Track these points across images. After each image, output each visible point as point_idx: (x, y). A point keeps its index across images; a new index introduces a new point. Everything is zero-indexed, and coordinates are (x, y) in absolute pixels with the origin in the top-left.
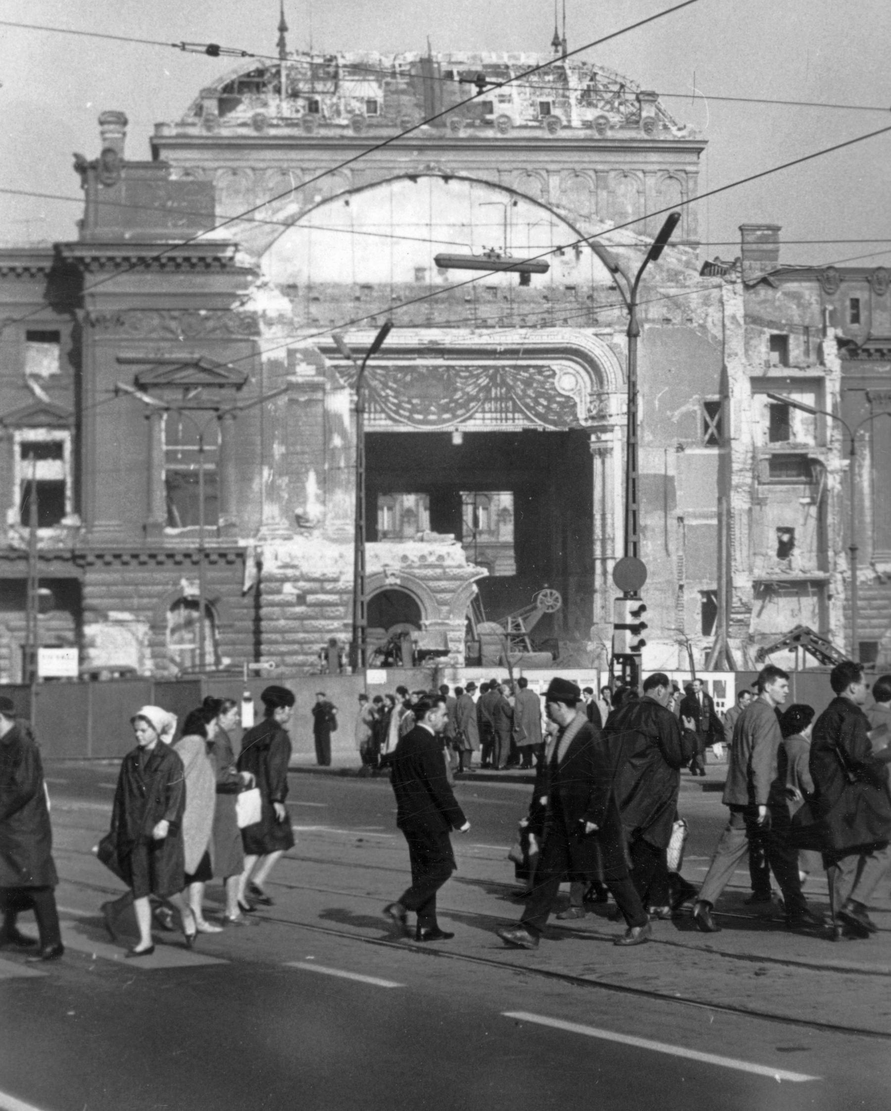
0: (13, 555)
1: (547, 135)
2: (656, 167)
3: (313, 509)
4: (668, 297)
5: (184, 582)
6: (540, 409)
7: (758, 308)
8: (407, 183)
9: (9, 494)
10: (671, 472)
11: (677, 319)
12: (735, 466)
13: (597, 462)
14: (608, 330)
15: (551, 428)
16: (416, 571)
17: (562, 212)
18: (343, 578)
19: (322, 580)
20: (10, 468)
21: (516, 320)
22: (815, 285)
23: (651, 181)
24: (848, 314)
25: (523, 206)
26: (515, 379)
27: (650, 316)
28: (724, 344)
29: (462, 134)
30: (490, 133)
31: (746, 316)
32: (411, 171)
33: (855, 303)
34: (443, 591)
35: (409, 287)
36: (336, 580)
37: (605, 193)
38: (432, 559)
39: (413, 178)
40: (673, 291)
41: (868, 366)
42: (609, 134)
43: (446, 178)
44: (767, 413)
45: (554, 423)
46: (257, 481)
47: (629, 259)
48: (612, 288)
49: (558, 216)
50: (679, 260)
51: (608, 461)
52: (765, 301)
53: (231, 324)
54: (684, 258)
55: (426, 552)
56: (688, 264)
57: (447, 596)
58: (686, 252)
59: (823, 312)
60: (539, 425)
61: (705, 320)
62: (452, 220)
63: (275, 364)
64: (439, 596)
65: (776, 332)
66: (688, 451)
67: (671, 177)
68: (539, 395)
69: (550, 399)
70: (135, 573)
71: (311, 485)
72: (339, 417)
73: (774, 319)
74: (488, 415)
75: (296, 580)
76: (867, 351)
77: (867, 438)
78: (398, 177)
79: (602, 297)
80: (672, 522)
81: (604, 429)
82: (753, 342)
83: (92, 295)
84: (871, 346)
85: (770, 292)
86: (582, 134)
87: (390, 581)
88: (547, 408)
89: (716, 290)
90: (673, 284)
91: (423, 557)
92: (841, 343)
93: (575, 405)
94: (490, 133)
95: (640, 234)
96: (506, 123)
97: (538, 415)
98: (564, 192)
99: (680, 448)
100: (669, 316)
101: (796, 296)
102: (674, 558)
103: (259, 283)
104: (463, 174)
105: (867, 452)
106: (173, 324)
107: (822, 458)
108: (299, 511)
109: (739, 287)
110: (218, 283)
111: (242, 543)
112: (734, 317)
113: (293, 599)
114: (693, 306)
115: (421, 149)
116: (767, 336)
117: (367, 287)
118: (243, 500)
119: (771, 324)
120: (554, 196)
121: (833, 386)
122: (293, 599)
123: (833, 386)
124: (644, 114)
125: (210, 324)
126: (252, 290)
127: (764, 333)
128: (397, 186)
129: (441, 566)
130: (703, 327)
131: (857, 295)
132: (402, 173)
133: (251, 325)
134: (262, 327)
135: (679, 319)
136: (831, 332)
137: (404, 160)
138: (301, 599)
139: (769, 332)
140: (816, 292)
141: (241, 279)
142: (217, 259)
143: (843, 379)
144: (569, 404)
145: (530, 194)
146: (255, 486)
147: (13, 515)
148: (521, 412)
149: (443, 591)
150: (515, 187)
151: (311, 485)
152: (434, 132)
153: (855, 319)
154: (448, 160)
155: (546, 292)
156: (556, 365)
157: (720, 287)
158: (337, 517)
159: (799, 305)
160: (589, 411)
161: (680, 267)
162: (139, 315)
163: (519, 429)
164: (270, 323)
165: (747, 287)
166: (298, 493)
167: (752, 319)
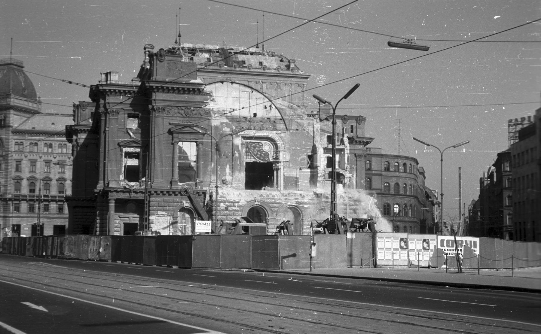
0: (125, 191)
1: (263, 71)
2: (295, 83)
3: (228, 178)
5: (184, 202)
6: (258, 156)
9: (121, 170)
10: (298, 176)
11: (300, 130)
12: (319, 175)
13: (275, 172)
14: (280, 132)
15: (261, 161)
16: (266, 200)
17: (267, 95)
18: (241, 202)
19: (234, 202)
20: (121, 161)
21: (252, 128)
22: (341, 121)
24: (350, 130)
25: (255, 93)
26: (251, 146)
28: (314, 137)
29: (238, 69)
30: (246, 70)
31: (320, 129)
32: (222, 80)
33: (352, 127)
34: (274, 207)
36: (238, 202)
38: (270, 196)
39: (222, 82)
40: (299, 121)
41: (356, 146)
42: (281, 72)
43: (232, 83)
44: (326, 159)
45: (262, 160)
46: (209, 167)
48: (281, 119)
49: (265, 96)
51: (279, 172)
53: (202, 113)
55: (268, 194)
56: (304, 113)
57: (276, 209)
59: (343, 129)
60: (258, 160)
63: (216, 127)
64: (273, 209)
65: (329, 134)
66: (303, 170)
68: (258, 151)
69: (261, 153)
70: (167, 198)
71: (228, 170)
72: (238, 146)
75: (224, 202)
76: (356, 141)
78: (217, 82)
79: (277, 121)
81: (278, 162)
83: (155, 100)
84: (358, 140)
85: (327, 122)
86: (273, 71)
87: (257, 203)
88: (260, 155)
91: (268, 195)
92: (349, 138)
93: (269, 155)
94: (246, 70)
96: (250, 67)
97: (257, 157)
98: (267, 89)
99: (301, 169)
103: (211, 99)
104: (237, 82)
105: (355, 172)
106: (182, 112)
107: (344, 173)
108: (223, 178)
109: (318, 120)
110: (198, 98)
111: (204, 189)
113: (224, 208)
115: (225, 73)
118: (205, 173)
119: (328, 132)
120: (264, 90)
121: (347, 151)
122: (224, 208)
123: (347, 151)
124: (291, 66)
125: (195, 112)
126: (209, 101)
128: (217, 85)
129: (273, 199)
130: (308, 132)
131: (353, 124)
132: (219, 80)
133: (208, 113)
134: (212, 114)
136: (346, 135)
137: (220, 77)
138: (227, 209)
139: (327, 135)
141: (205, 97)
142: (199, 89)
143: (350, 150)
144: (267, 155)
145: (257, 89)
146: (209, 169)
147: (122, 177)
148: (252, 156)
149: (274, 207)
150: (253, 87)
151: (228, 170)
152: (229, 68)
153: (352, 131)
154: (233, 77)
155: (261, 120)
156: (263, 142)
157: (313, 120)
158: (236, 181)
160: (273, 157)
162: (170, 108)
163: (252, 161)
164: (214, 113)
165: (321, 120)
166: (224, 171)
167: (322, 130)
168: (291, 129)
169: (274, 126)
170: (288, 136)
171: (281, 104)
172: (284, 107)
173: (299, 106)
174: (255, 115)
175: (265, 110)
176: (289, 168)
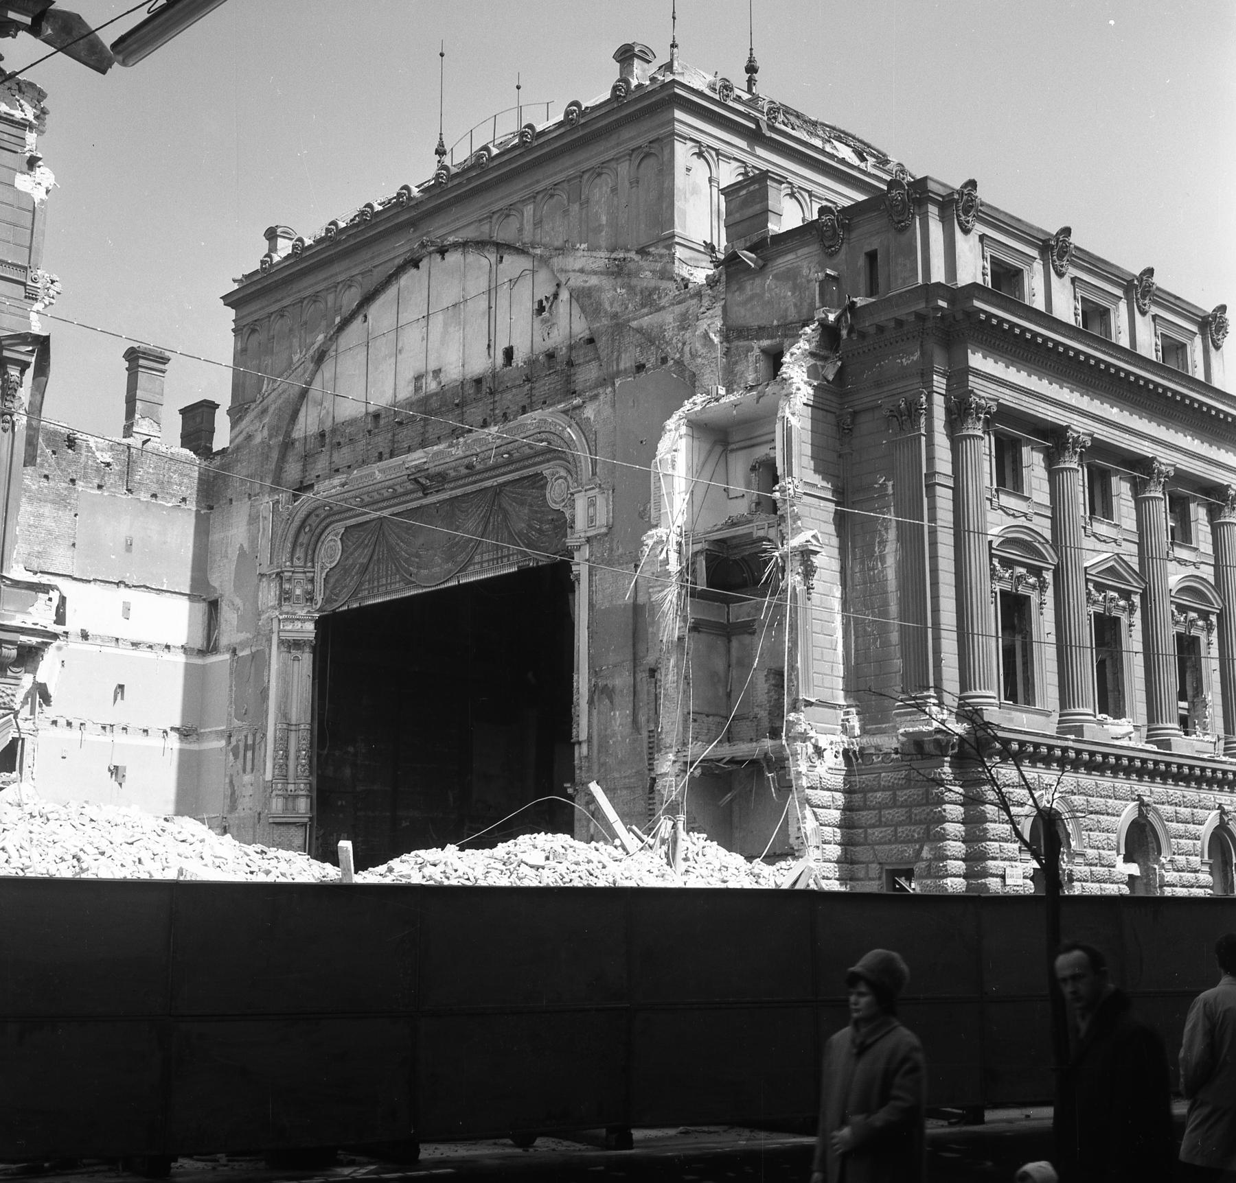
4: (639, 330)
7: (743, 312)
8: (413, 271)
23: (624, 168)
27: (622, 367)
35: (410, 404)
37: (576, 207)
40: (646, 321)
43: (442, 252)
47: (599, 289)
52: (751, 298)
54: (659, 266)
58: (661, 256)
61: (682, 352)
65: (765, 343)
67: (648, 155)
73: (763, 323)
74: (486, 557)
77: (890, 491)
80: (643, 676)
82: (738, 368)
89: (694, 301)
90: (645, 310)
95: (612, 252)
100: (642, 360)
101: (790, 276)
102: (645, 734)
114: (668, 335)
116: (757, 352)
117: (376, 416)
119: (761, 332)
127: (751, 349)
135: (653, 360)
137: (401, 247)
159: (794, 289)
161: (653, 283)
167: (732, 333)
168: (618, 374)
169: (569, 380)
170: (607, 411)
171: (582, 271)
172: (594, 281)
173: (643, 252)
174: (509, 353)
175: (538, 320)
176: (610, 563)
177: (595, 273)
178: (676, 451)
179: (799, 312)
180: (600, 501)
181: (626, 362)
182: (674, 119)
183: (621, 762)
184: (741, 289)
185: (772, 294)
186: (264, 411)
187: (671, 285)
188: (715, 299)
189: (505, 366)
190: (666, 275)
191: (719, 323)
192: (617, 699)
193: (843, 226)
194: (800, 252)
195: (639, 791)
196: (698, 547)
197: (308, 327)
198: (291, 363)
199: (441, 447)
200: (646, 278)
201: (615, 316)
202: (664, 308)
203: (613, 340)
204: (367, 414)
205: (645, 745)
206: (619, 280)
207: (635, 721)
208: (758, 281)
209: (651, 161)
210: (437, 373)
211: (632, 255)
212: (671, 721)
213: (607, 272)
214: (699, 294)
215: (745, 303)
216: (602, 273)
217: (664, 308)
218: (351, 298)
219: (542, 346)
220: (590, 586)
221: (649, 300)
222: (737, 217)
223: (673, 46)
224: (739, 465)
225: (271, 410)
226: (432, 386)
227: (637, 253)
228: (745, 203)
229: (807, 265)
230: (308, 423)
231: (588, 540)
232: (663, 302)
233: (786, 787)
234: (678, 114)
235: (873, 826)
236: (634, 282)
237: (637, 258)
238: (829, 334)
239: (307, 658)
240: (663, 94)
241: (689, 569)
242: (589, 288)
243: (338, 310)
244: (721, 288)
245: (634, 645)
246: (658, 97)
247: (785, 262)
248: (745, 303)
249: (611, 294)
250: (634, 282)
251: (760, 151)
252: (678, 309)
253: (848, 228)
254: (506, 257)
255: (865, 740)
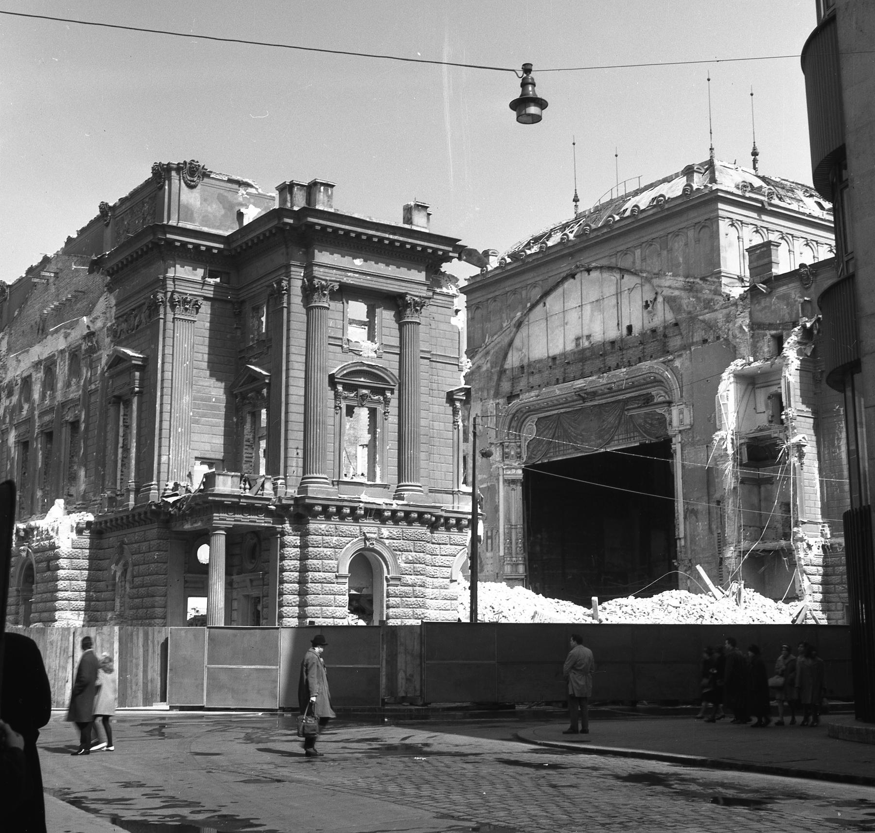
4: (703, 321)
8: (572, 280)
23: (691, 233)
27: (695, 340)
35: (573, 353)
37: (665, 252)
39: (573, 276)
40: (707, 316)
43: (589, 271)
47: (681, 298)
50: (710, 290)
52: (765, 308)
54: (713, 288)
58: (714, 282)
61: (728, 334)
62: (591, 300)
65: (773, 332)
67: (704, 227)
73: (772, 321)
74: (621, 437)
80: (713, 505)
82: (758, 345)
90: (706, 311)
95: (687, 277)
100: (706, 337)
101: (785, 298)
102: (716, 535)
112: (741, 327)
114: (720, 325)
116: (769, 337)
117: (554, 358)
119: (770, 326)
135: (712, 337)
137: (565, 267)
140: (799, 290)
159: (788, 304)
161: (710, 297)
167: (755, 326)
168: (693, 344)
169: (665, 345)
170: (687, 363)
171: (670, 287)
172: (677, 293)
173: (703, 279)
174: (630, 328)
175: (645, 312)
176: (693, 444)
177: (677, 289)
178: (728, 391)
179: (791, 317)
180: (686, 411)
181: (697, 338)
182: (718, 209)
183: (704, 549)
184: (759, 303)
185: (777, 307)
186: (487, 353)
187: (720, 298)
188: (744, 307)
189: (628, 335)
190: (717, 292)
191: (748, 321)
192: (699, 516)
193: (813, 274)
194: (790, 285)
195: (714, 565)
196: (742, 441)
197: (512, 308)
198: (502, 328)
199: (594, 378)
200: (706, 294)
201: (689, 313)
202: (716, 310)
203: (689, 326)
204: (549, 357)
205: (716, 541)
206: (691, 294)
207: (710, 528)
208: (768, 299)
209: (706, 229)
210: (588, 337)
211: (698, 280)
212: (731, 531)
213: (684, 289)
214: (735, 304)
215: (761, 311)
216: (681, 289)
217: (716, 310)
218: (536, 293)
219: (648, 326)
220: (682, 456)
221: (708, 305)
222: (755, 264)
223: (711, 149)
224: (761, 396)
225: (492, 352)
226: (586, 344)
227: (701, 279)
228: (759, 257)
229: (792, 290)
230: (513, 360)
231: (680, 432)
232: (716, 307)
233: (793, 565)
234: (720, 206)
235: (838, 584)
236: (700, 295)
237: (701, 282)
238: (807, 333)
239: (519, 488)
240: (713, 195)
241: (738, 452)
242: (675, 297)
243: (529, 300)
244: (748, 301)
245: (708, 488)
246: (709, 197)
247: (782, 290)
248: (761, 311)
249: (687, 301)
250: (700, 295)
251: (764, 217)
252: (725, 311)
253: (815, 275)
254: (625, 276)
255: (833, 540)
